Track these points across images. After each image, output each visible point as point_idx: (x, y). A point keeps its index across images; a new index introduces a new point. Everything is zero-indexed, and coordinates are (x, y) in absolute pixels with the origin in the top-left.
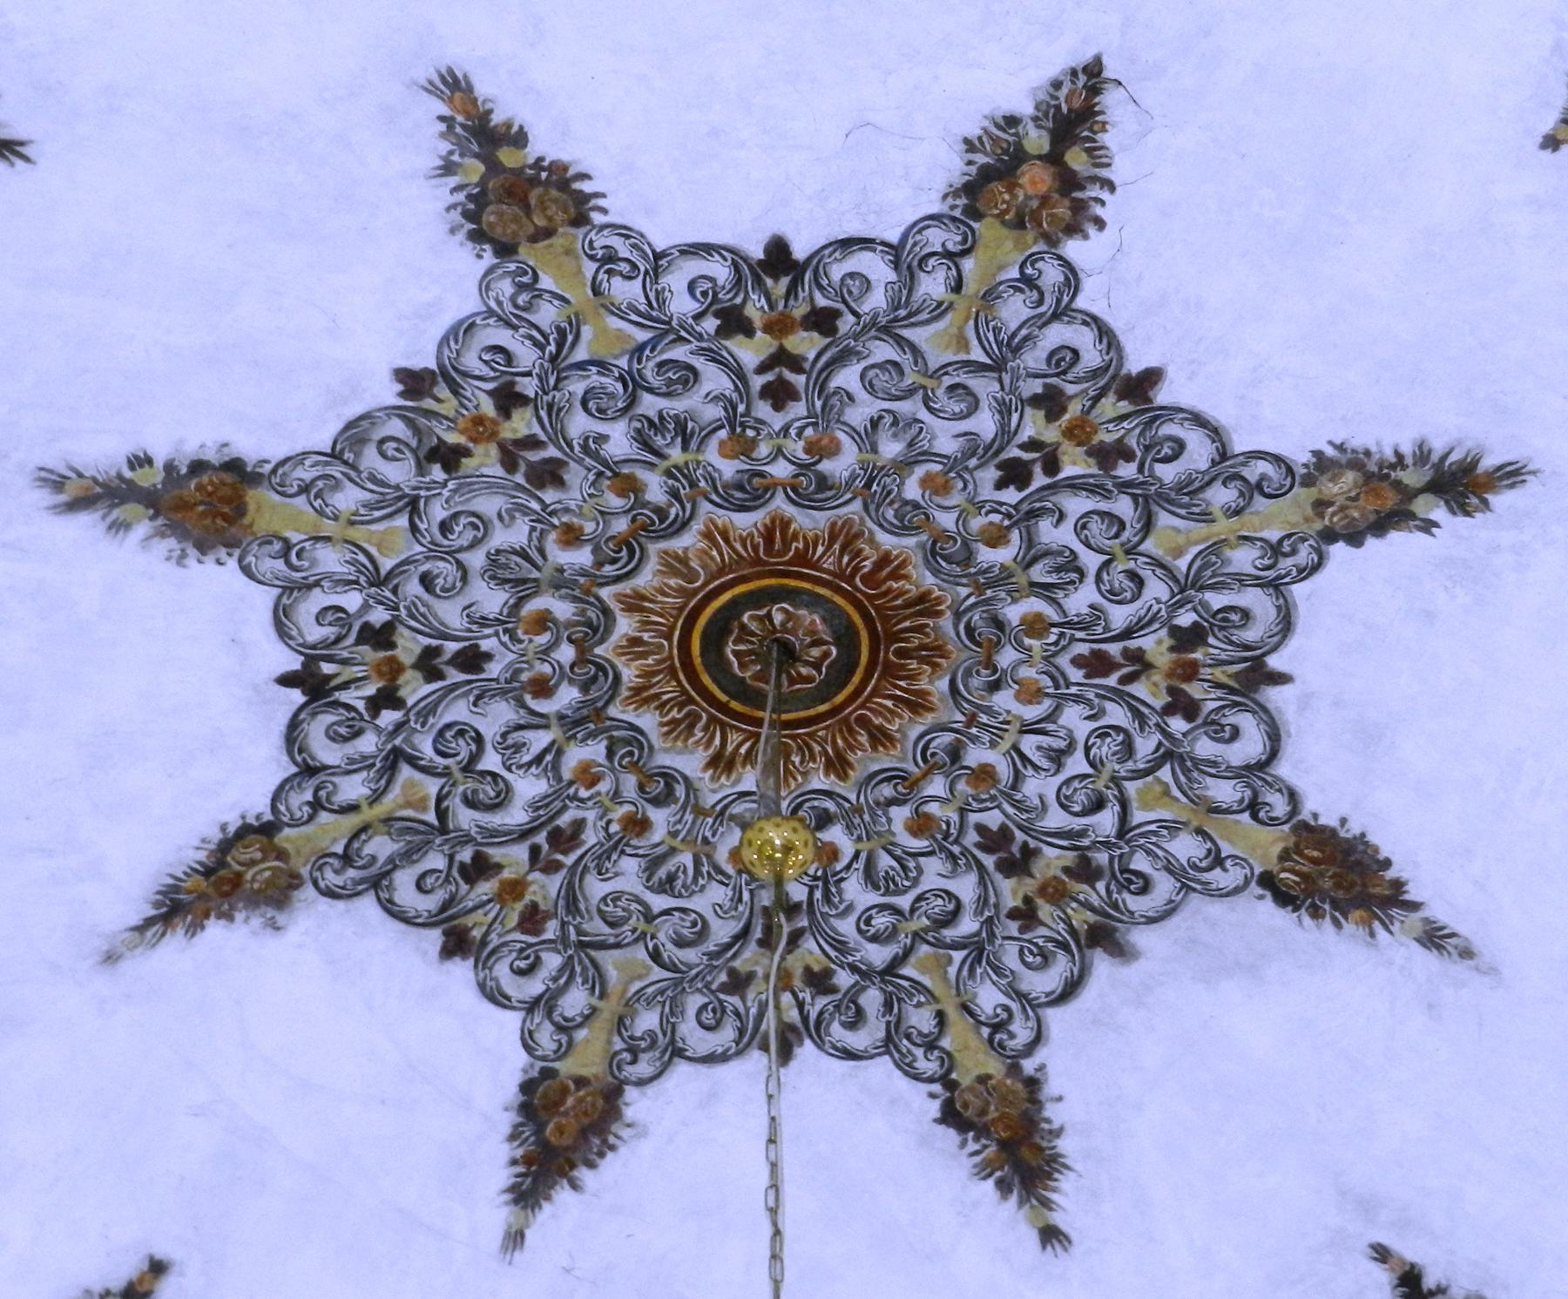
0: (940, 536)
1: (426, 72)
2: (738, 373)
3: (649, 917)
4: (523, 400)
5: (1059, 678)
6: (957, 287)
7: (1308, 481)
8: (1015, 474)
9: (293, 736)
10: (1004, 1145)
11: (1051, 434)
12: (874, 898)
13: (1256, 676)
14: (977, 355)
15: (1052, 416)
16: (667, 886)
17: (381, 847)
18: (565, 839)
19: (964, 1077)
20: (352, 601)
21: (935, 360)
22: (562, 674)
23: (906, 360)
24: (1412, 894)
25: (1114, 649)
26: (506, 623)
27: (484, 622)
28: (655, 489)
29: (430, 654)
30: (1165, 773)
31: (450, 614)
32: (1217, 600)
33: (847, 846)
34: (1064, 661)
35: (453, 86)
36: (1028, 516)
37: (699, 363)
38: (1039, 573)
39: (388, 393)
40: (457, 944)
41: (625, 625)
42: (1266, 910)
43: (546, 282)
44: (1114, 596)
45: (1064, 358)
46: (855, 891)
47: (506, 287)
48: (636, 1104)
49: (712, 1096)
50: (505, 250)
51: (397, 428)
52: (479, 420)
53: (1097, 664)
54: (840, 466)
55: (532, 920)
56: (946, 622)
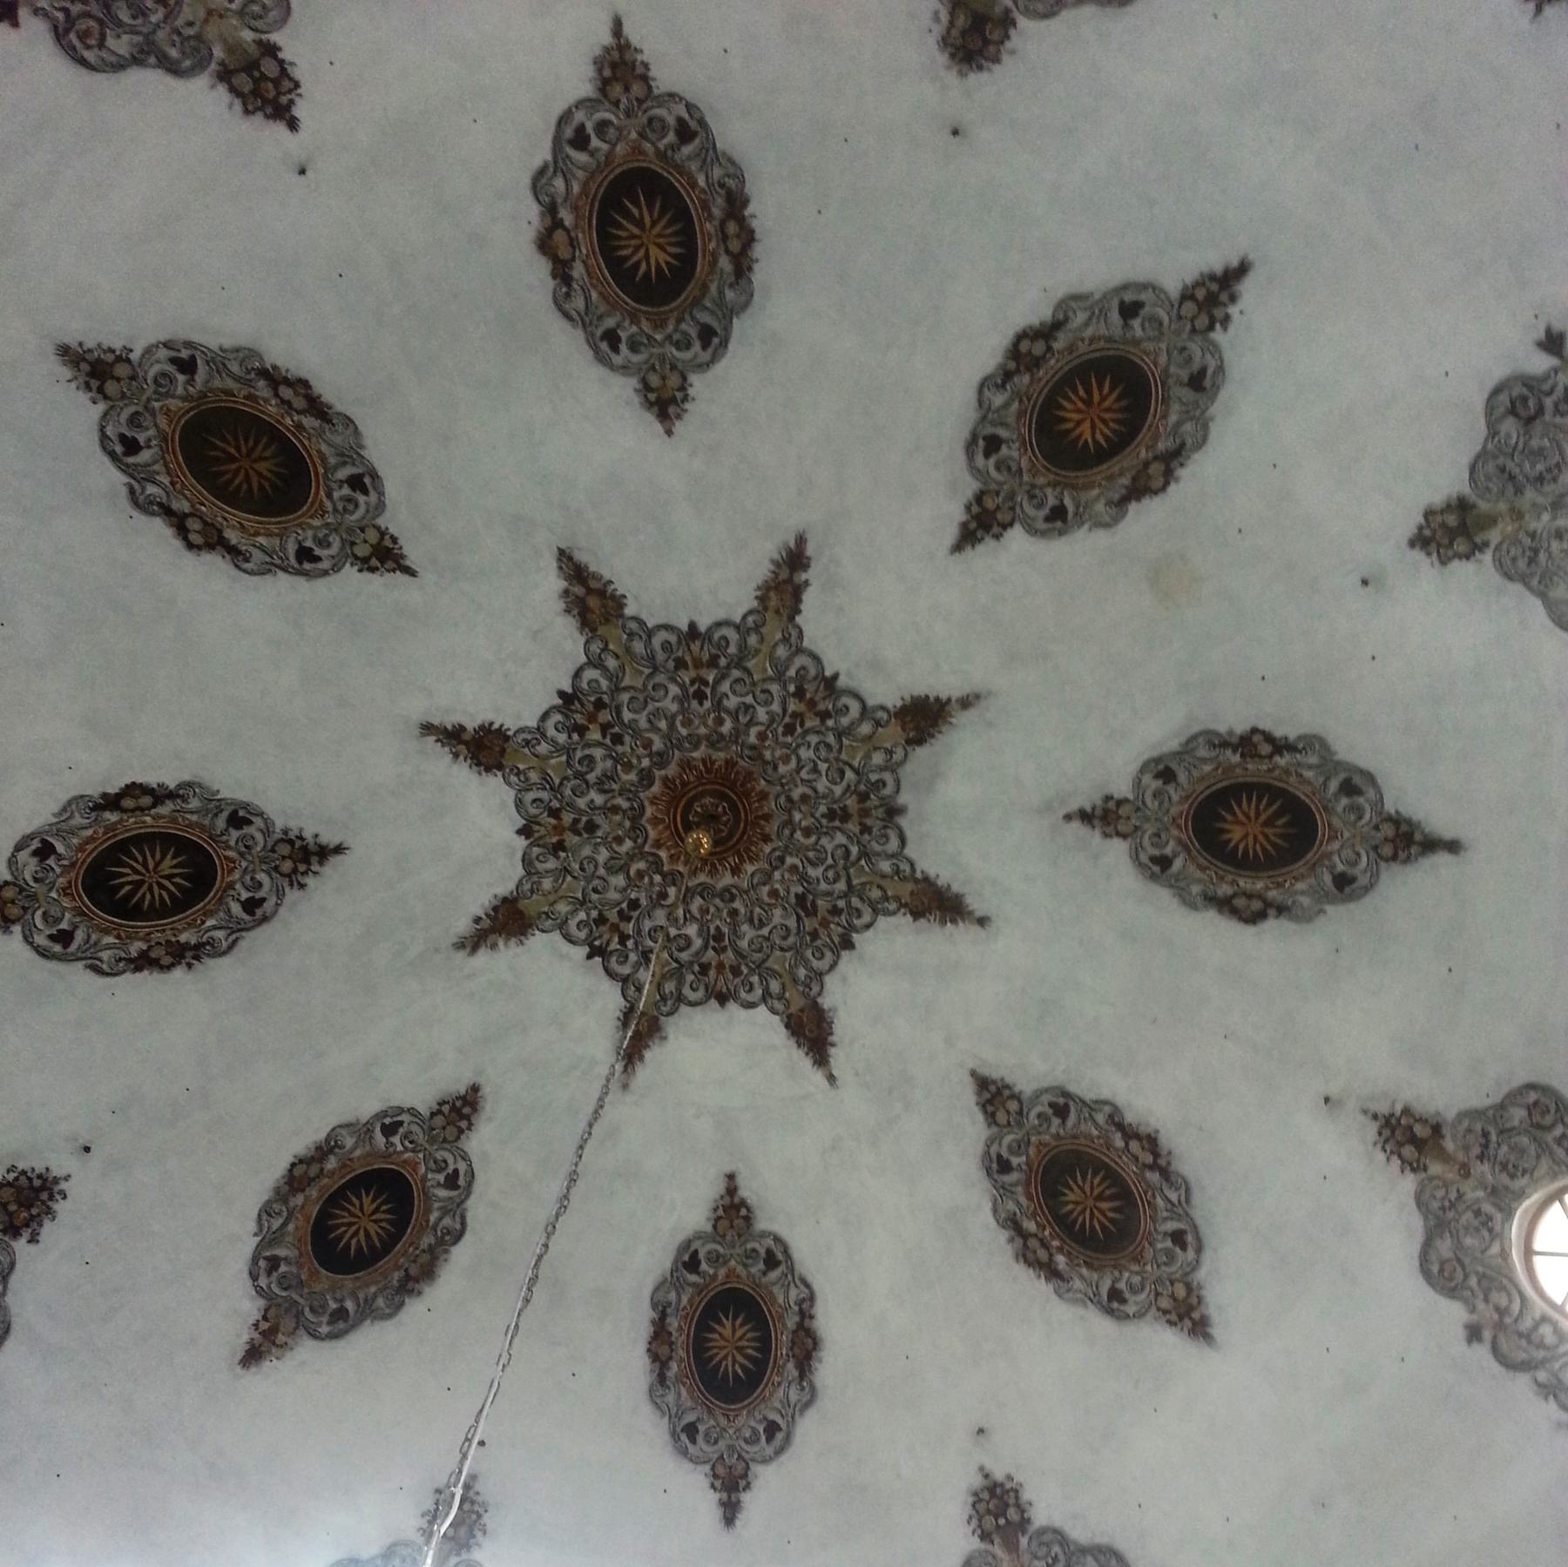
0: (707, 738)
1: (417, 732)
2: (599, 744)
3: (767, 939)
4: (559, 810)
5: (788, 746)
6: (617, 657)
7: (766, 609)
8: (700, 696)
9: (610, 974)
10: (940, 908)
11: (693, 673)
12: (821, 869)
13: (830, 683)
14: (647, 671)
15: (687, 668)
16: (762, 925)
17: (670, 987)
18: (719, 936)
19: (906, 899)
20: (582, 915)
21: (639, 684)
22: (664, 885)
23: (632, 693)
24: (944, 697)
25: (787, 720)
26: (632, 883)
27: (625, 889)
28: (621, 802)
29: (621, 913)
30: (845, 742)
31: (613, 895)
32: (792, 672)
33: (796, 861)
34: (781, 739)
35: (428, 728)
36: (718, 706)
37: (587, 752)
38: (743, 719)
39: (522, 843)
40: (722, 999)
41: (663, 854)
42: (921, 753)
43: (521, 767)
44: (767, 703)
45: (666, 646)
46: (814, 873)
47: (513, 779)
48: (826, 1002)
49: (844, 979)
50: (500, 767)
51: (536, 850)
52: (555, 827)
53: (789, 729)
54: (658, 745)
55: (736, 971)
56: (741, 763)
